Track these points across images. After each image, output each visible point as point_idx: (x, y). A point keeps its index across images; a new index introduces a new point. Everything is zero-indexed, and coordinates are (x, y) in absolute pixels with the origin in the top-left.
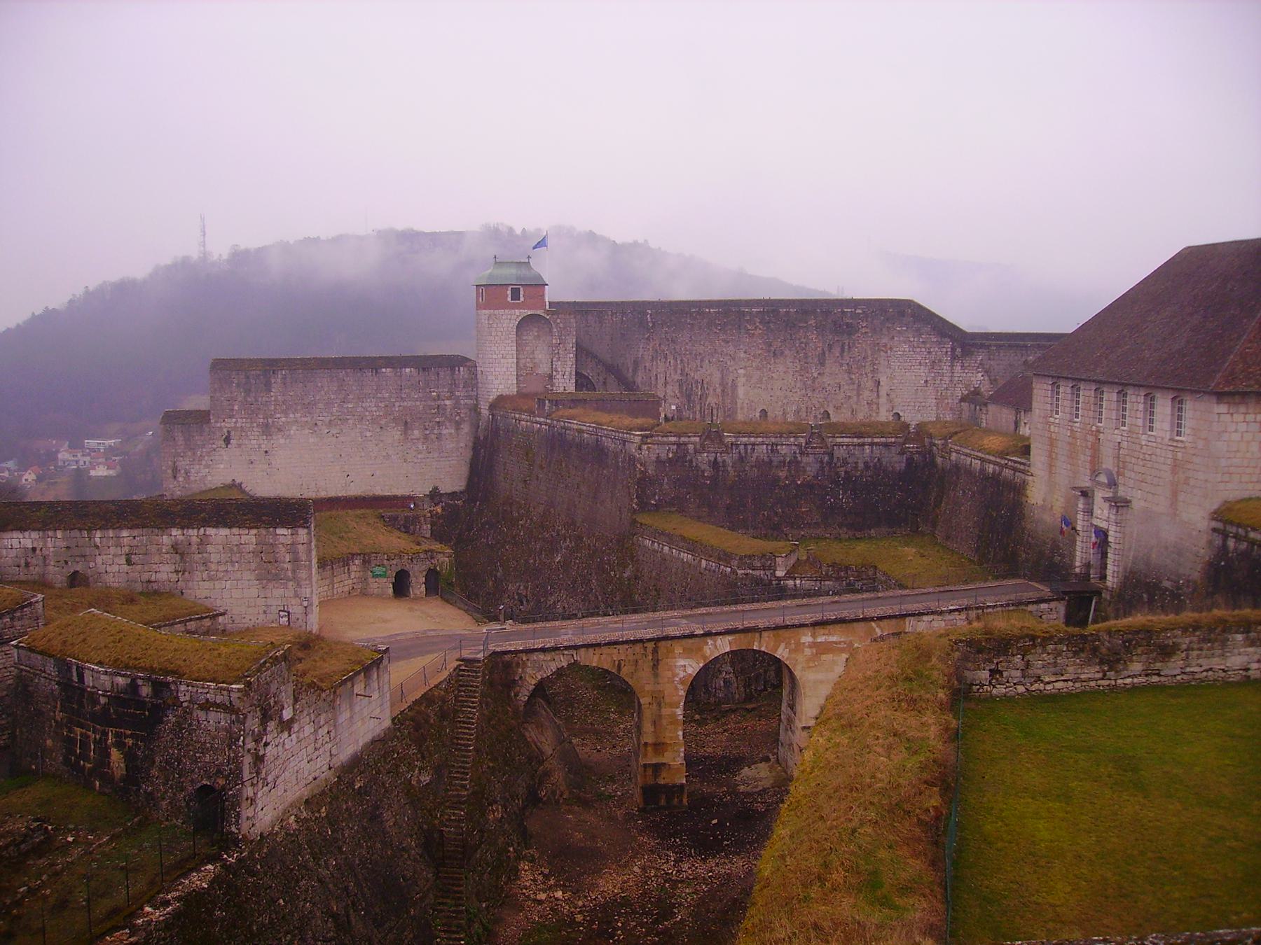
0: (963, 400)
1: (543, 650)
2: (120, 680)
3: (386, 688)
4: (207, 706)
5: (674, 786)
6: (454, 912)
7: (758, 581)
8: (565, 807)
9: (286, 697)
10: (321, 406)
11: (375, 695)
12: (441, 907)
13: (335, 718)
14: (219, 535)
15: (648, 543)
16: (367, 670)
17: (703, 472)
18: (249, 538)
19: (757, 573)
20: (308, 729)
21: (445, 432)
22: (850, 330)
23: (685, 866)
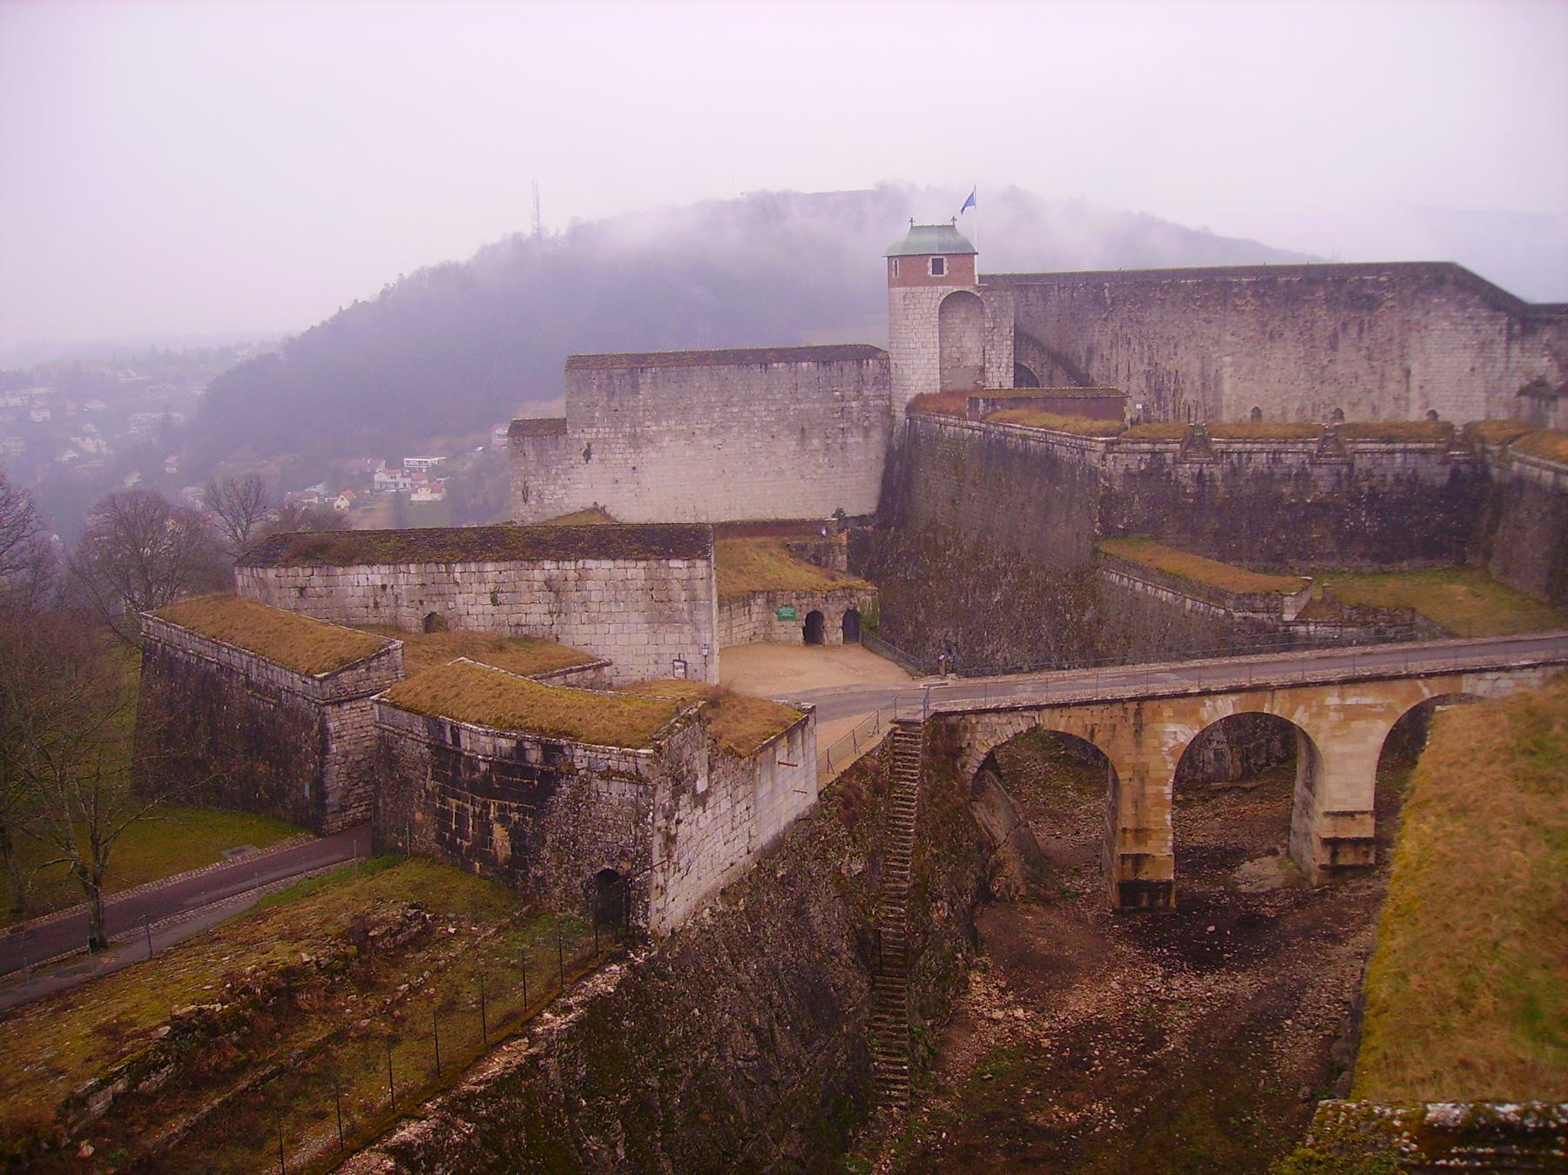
0: (1522, 392)
1: (997, 711)
2: (504, 743)
3: (812, 756)
4: (608, 775)
5: (1160, 883)
6: (893, 1030)
7: (1260, 627)
8: (1021, 907)
9: (700, 766)
10: (700, 411)
11: (801, 764)
12: (879, 1024)
13: (754, 792)
14: (600, 568)
15: (1115, 578)
16: (790, 733)
17: (1184, 488)
18: (636, 571)
19: (1259, 616)
20: (725, 805)
21: (850, 440)
22: (1371, 303)
23: (1176, 983)
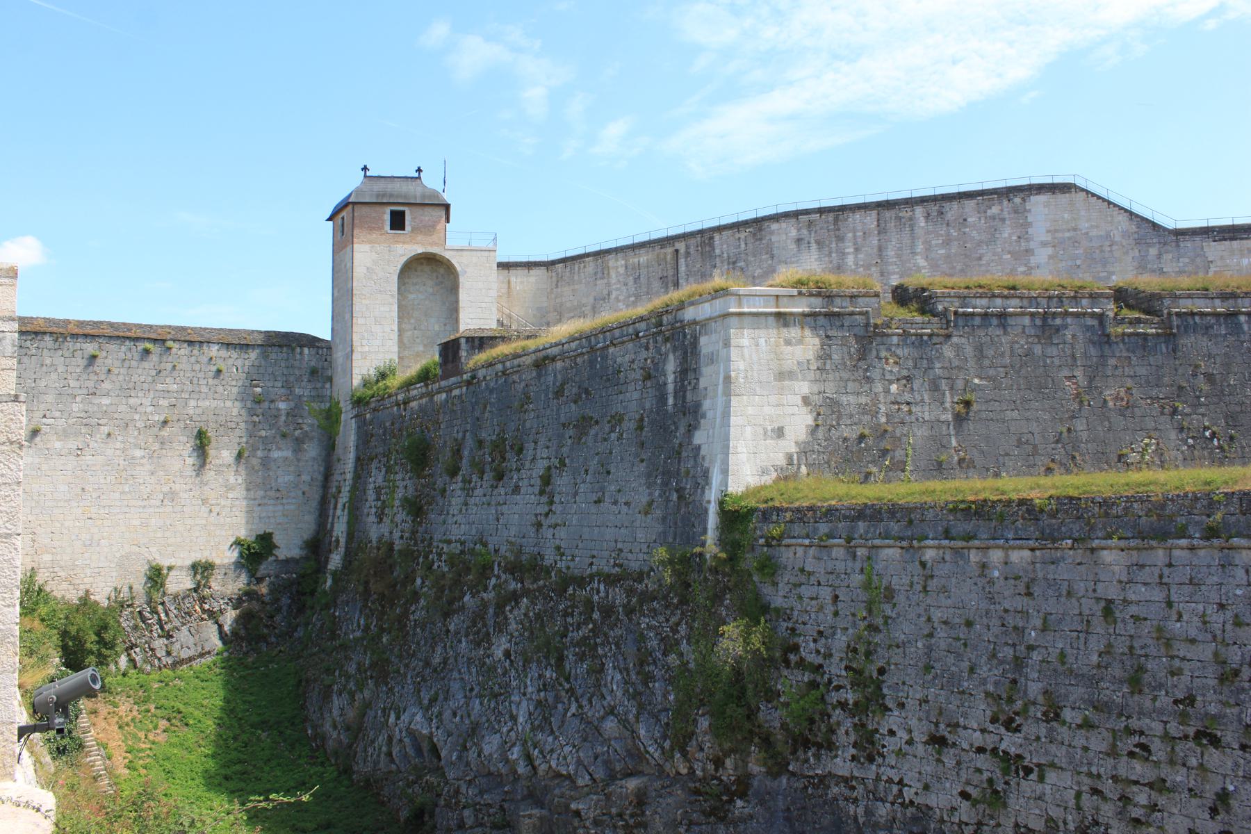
10: (50, 398)
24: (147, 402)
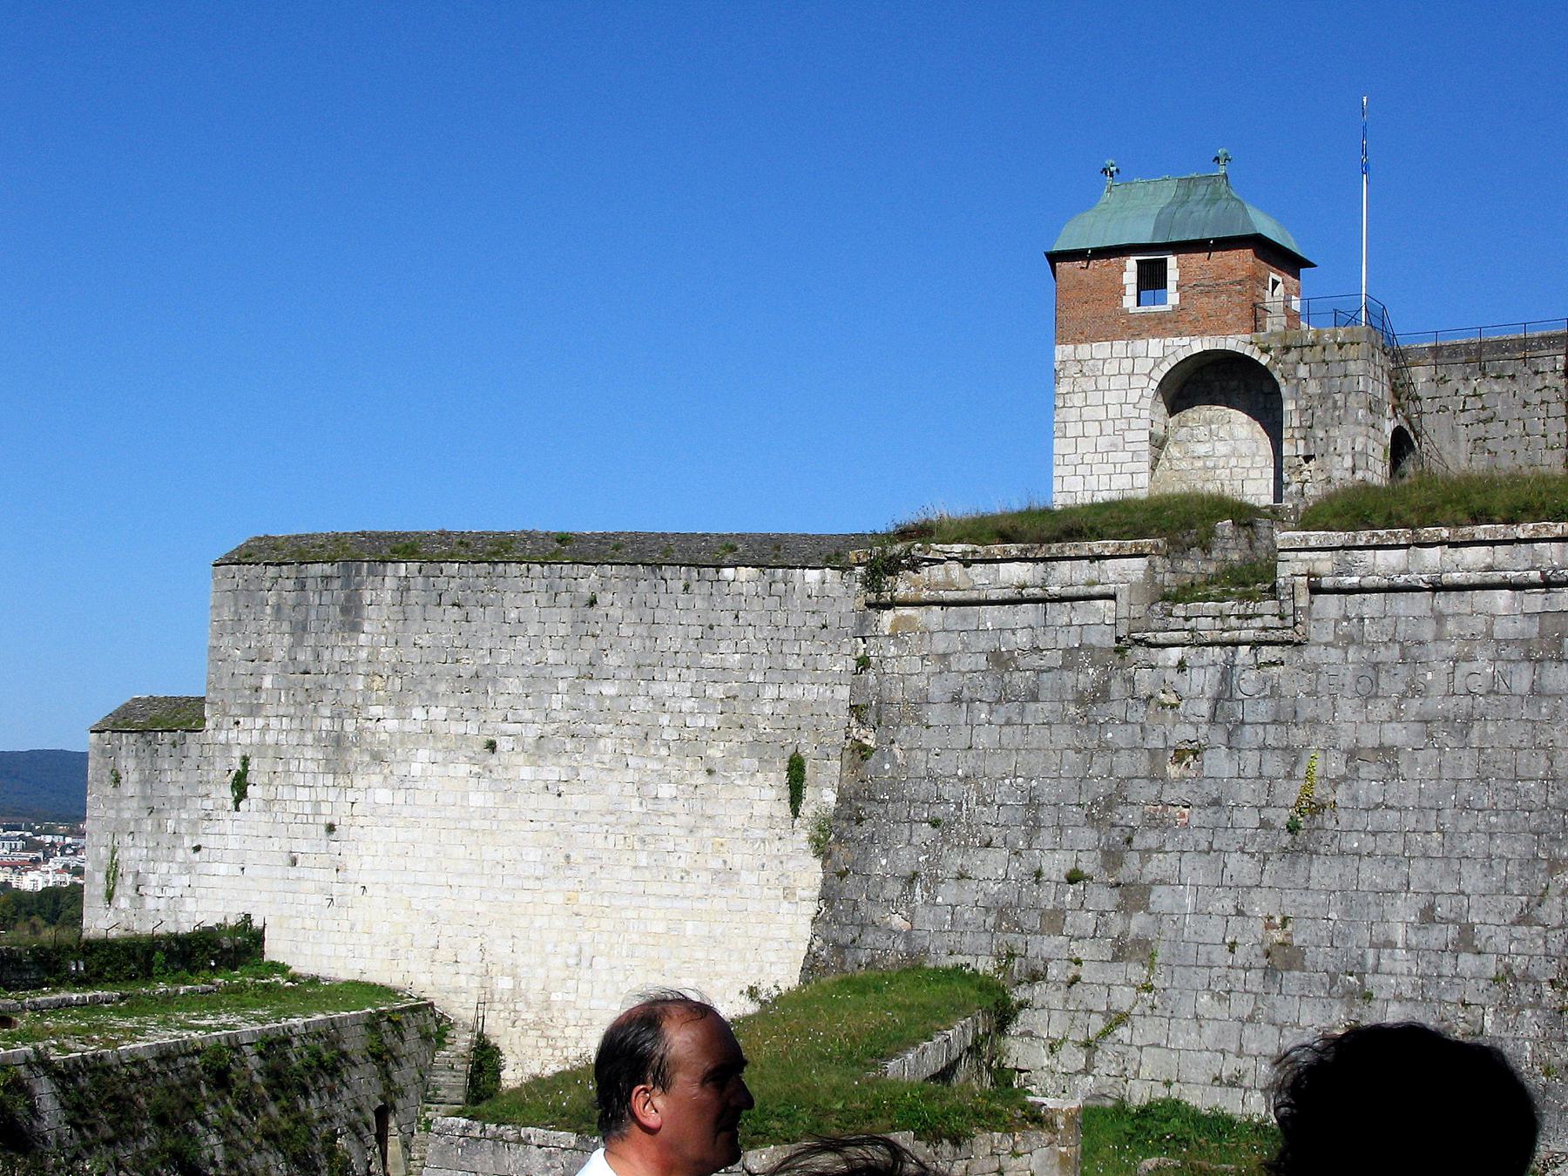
10: (514, 685)
24: (684, 689)
